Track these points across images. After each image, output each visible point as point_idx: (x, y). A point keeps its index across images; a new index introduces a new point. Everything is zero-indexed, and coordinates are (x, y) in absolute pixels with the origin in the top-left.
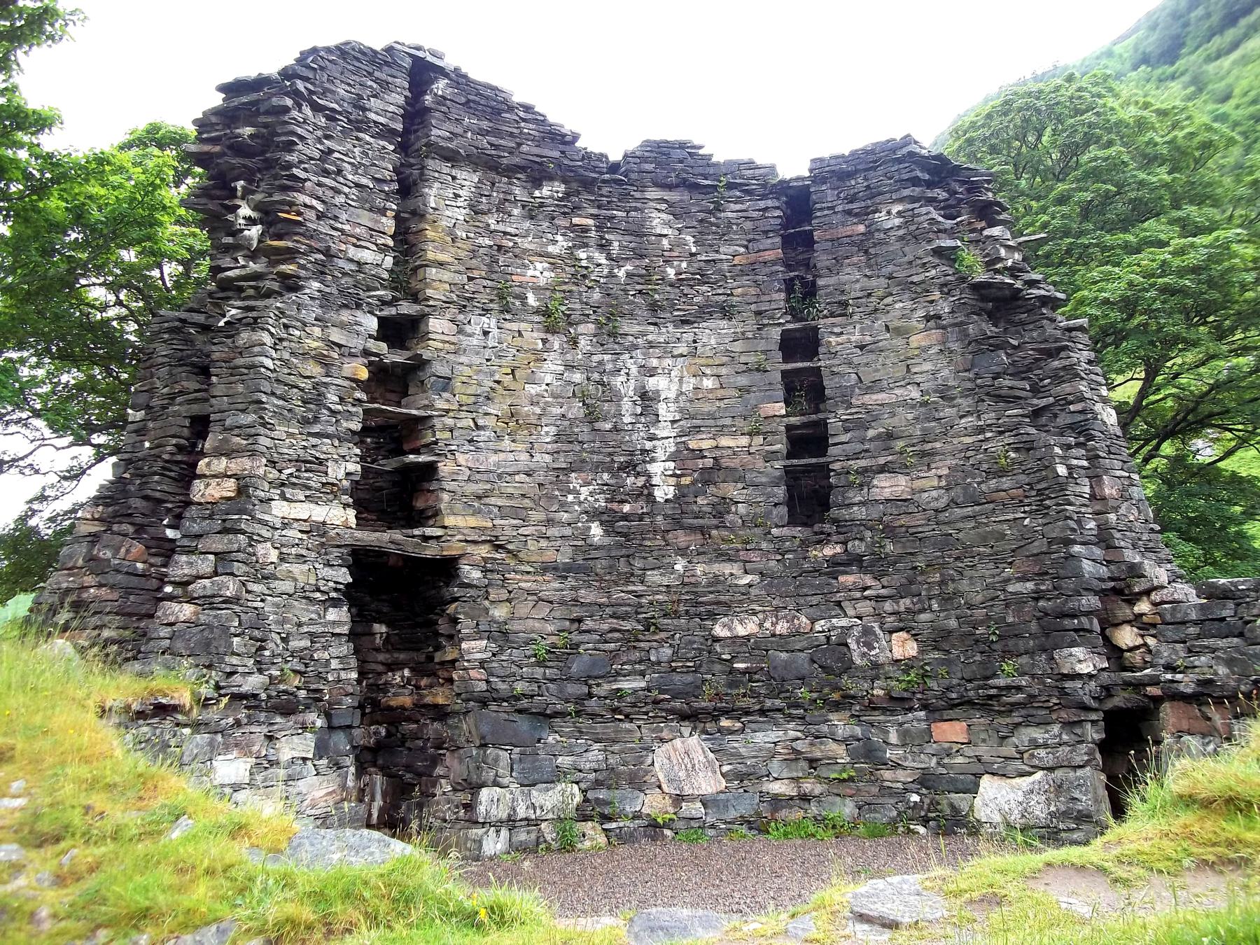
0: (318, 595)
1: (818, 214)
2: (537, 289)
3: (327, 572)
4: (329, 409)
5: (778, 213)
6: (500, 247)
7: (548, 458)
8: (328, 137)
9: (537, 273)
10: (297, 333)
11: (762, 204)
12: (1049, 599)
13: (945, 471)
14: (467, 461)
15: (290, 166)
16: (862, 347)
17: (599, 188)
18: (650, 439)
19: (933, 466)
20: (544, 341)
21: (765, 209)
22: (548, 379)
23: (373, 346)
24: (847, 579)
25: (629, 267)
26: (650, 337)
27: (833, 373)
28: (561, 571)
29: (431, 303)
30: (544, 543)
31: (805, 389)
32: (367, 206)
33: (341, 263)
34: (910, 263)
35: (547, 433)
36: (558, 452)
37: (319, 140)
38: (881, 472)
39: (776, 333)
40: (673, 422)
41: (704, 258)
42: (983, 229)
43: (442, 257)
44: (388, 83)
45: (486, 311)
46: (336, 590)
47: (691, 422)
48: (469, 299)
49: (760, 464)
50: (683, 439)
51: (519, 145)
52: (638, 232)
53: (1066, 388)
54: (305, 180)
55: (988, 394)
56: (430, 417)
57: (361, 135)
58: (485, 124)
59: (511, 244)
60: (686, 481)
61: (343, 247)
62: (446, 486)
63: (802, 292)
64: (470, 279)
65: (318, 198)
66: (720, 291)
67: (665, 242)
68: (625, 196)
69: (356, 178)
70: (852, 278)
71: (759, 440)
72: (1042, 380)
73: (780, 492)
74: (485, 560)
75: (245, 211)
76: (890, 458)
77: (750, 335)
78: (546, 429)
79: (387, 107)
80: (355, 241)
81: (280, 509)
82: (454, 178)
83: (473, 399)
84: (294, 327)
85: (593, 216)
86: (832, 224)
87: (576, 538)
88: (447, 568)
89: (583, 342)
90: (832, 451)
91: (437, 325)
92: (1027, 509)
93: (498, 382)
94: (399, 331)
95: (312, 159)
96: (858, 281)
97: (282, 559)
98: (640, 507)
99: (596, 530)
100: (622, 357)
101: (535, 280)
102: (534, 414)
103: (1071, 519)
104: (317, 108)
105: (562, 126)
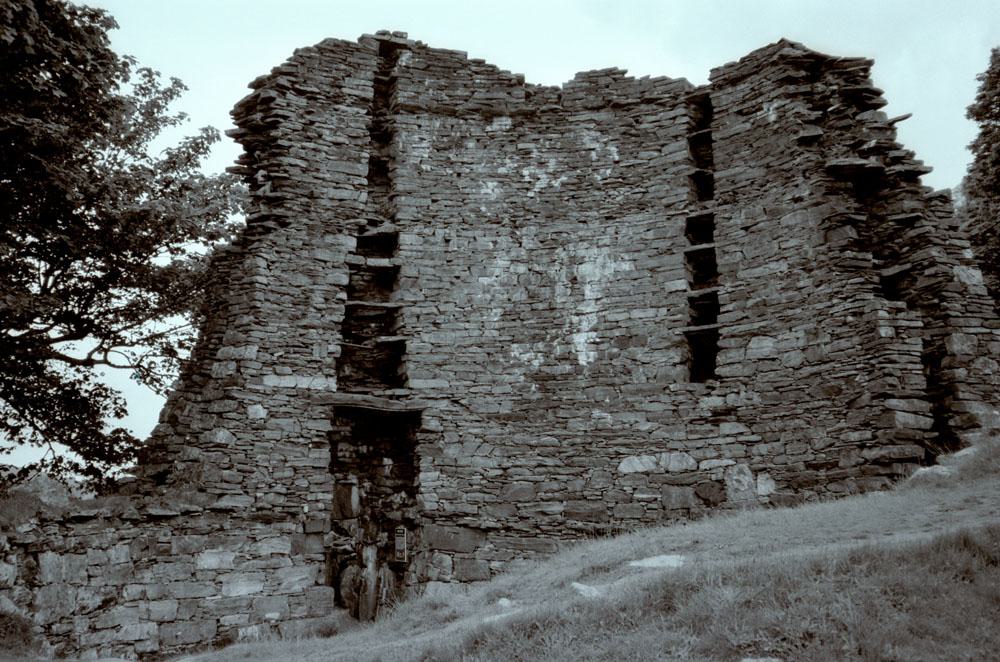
0: (301, 440)
1: (716, 117)
2: (489, 204)
3: (311, 424)
4: (315, 308)
5: (686, 119)
6: (459, 175)
7: (496, 333)
8: (309, 113)
9: (490, 191)
10: (288, 256)
11: (672, 114)
12: (870, 448)
13: (801, 334)
14: (430, 338)
15: (276, 139)
16: (746, 229)
17: (540, 118)
18: (577, 314)
19: (793, 330)
20: (495, 243)
21: (674, 118)
22: (497, 271)
24: (727, 428)
25: (564, 178)
26: (580, 233)
27: (725, 253)
28: (503, 420)
29: (402, 222)
30: (489, 399)
31: (703, 268)
32: (345, 158)
33: (323, 202)
34: (782, 152)
35: (496, 314)
36: (504, 328)
37: (302, 117)
38: (755, 335)
39: (681, 222)
40: (597, 300)
41: (624, 164)
42: (855, 114)
43: (408, 187)
44: (359, 65)
45: (447, 224)
46: (317, 436)
48: (434, 217)
49: (665, 332)
50: (604, 313)
51: (473, 92)
53: (919, 255)
54: (290, 147)
55: (836, 265)
56: (401, 307)
57: (337, 106)
58: (443, 82)
59: (468, 170)
60: (602, 347)
61: (325, 190)
62: (410, 357)
64: (434, 201)
65: (302, 158)
66: (637, 190)
67: (593, 154)
68: (561, 121)
69: (333, 139)
71: (664, 311)
72: (901, 248)
74: (442, 411)
76: (762, 324)
77: (659, 225)
78: (494, 310)
79: (361, 85)
80: (334, 184)
81: (271, 381)
82: (420, 126)
83: (436, 292)
84: (284, 252)
85: (536, 140)
86: (728, 127)
87: (515, 395)
88: (414, 418)
89: (525, 241)
90: (721, 318)
91: (405, 239)
92: (858, 366)
93: (458, 278)
94: (372, 244)
95: (294, 130)
96: (744, 172)
97: (272, 415)
100: (557, 251)
101: (487, 196)
102: (486, 300)
103: (891, 375)
104: (300, 93)
105: (509, 72)
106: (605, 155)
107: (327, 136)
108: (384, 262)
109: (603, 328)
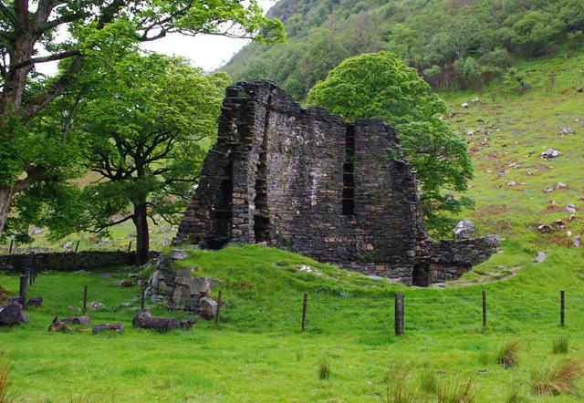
31: (349, 180)
47: (322, 185)
52: (310, 131)
63: (351, 151)
70: (363, 152)
73: (341, 206)
75: (234, 125)
86: (360, 137)
91: (268, 156)
99: (298, 212)
106: (321, 136)
109: (318, 193)
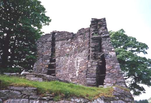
23: (49, 63)
52: (77, 42)
58: (61, 36)
79: (50, 39)
98: (75, 77)
106: (81, 42)
107: (45, 47)
108: (54, 63)
